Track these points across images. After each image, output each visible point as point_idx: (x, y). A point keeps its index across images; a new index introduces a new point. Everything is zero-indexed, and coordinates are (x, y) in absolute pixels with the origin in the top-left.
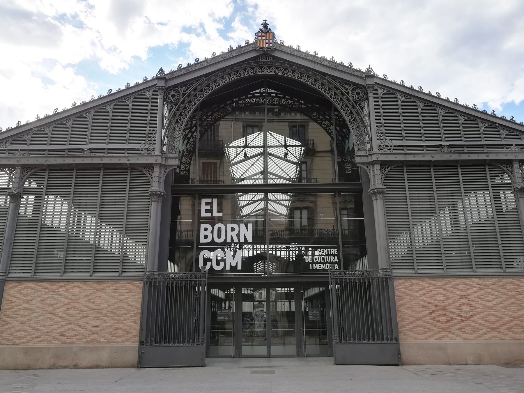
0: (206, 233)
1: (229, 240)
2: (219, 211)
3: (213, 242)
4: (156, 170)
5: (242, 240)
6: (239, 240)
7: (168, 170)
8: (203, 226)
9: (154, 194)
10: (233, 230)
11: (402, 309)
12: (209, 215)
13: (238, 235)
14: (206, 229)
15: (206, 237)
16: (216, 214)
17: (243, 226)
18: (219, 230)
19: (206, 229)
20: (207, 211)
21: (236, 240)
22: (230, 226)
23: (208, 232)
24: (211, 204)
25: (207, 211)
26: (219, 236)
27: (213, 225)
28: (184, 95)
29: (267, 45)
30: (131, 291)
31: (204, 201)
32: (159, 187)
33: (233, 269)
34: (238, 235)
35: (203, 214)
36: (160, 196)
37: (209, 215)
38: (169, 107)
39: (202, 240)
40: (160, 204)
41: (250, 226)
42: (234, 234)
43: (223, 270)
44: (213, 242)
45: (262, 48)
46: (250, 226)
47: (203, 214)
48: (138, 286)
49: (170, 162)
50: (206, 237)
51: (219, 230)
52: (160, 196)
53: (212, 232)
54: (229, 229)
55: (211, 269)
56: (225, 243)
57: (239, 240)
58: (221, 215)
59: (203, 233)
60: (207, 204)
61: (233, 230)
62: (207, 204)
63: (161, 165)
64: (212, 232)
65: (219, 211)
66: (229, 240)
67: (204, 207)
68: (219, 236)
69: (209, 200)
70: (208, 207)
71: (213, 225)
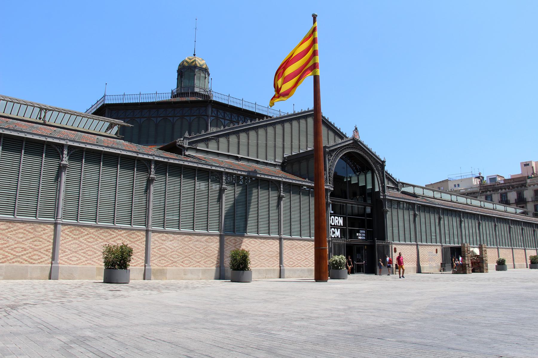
22: (336, 217)
33: (338, 237)
42: (337, 221)
43: (335, 237)
56: (334, 225)
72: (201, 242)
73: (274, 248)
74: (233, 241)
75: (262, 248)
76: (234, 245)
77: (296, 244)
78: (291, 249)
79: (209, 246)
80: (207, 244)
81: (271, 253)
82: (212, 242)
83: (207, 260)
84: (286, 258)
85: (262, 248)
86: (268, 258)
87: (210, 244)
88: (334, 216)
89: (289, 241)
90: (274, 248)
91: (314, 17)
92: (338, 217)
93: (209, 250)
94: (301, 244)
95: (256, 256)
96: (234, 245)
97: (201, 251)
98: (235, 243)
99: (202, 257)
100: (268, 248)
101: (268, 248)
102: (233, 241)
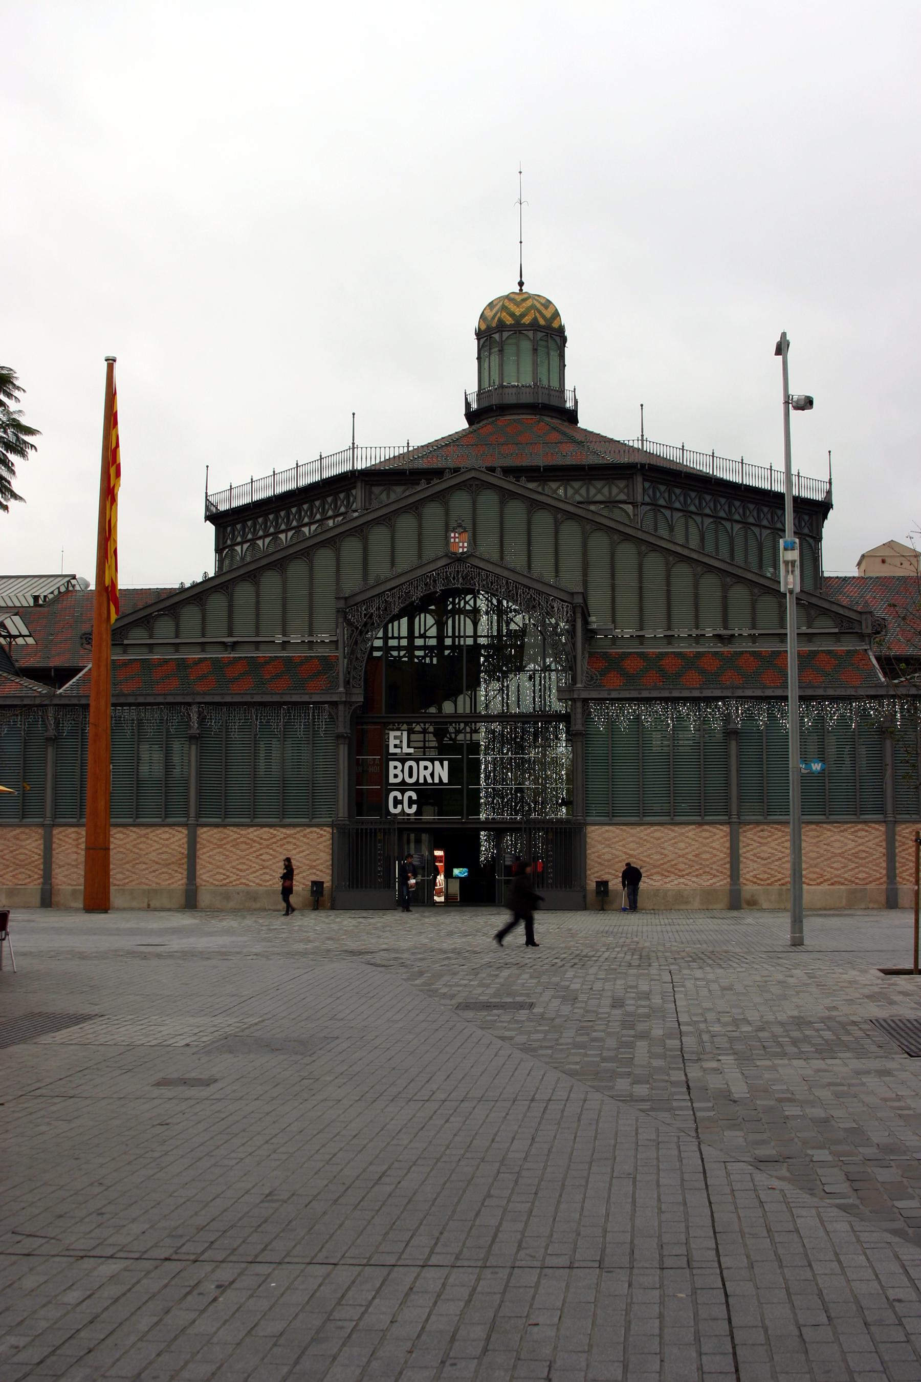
0: (396, 772)
1: (421, 781)
2: (409, 747)
3: (403, 782)
4: (341, 707)
5: (437, 781)
6: (433, 779)
7: (353, 708)
8: (392, 764)
9: (339, 737)
10: (426, 768)
11: (593, 857)
12: (398, 751)
13: (432, 775)
14: (395, 767)
15: (396, 776)
16: (406, 750)
17: (437, 763)
18: (411, 768)
19: (395, 767)
20: (396, 746)
21: (430, 781)
23: (398, 771)
24: (400, 738)
25: (396, 746)
26: (411, 776)
27: (403, 761)
28: (365, 615)
29: (461, 550)
30: (322, 836)
31: (392, 734)
32: (345, 727)
34: (432, 775)
35: (392, 750)
36: (345, 738)
37: (398, 751)
38: (350, 632)
39: (392, 780)
40: (346, 746)
41: (446, 763)
44: (403, 782)
45: (455, 554)
46: (446, 763)
47: (392, 750)
48: (328, 832)
49: (354, 699)
50: (396, 776)
51: (411, 768)
52: (345, 738)
53: (402, 771)
54: (421, 768)
55: (403, 812)
56: (417, 783)
57: (433, 779)
58: (411, 751)
59: (392, 772)
60: (396, 737)
61: (426, 768)
62: (396, 737)
63: (345, 702)
64: (402, 771)
65: (409, 747)
66: (421, 781)
67: (392, 742)
68: (411, 776)
69: (398, 733)
70: (397, 742)
71: (403, 761)
72: (5, 839)
73: (173, 846)
74: (73, 836)
75: (141, 846)
76: (75, 843)
77: (236, 836)
78: (220, 846)
79: (21, 847)
80: (18, 842)
81: (164, 856)
82: (27, 839)
83: (17, 871)
84: (205, 867)
85: (141, 846)
86: (157, 867)
87: (24, 843)
88: (417, 761)
89: (215, 830)
90: (173, 846)
91: (111, 363)
92: (432, 761)
93: (21, 854)
94: (251, 836)
95: (127, 863)
96: (75, 843)
97: (6, 857)
98: (77, 840)
99: (8, 866)
100: (157, 846)
101: (157, 846)
102: (73, 836)
